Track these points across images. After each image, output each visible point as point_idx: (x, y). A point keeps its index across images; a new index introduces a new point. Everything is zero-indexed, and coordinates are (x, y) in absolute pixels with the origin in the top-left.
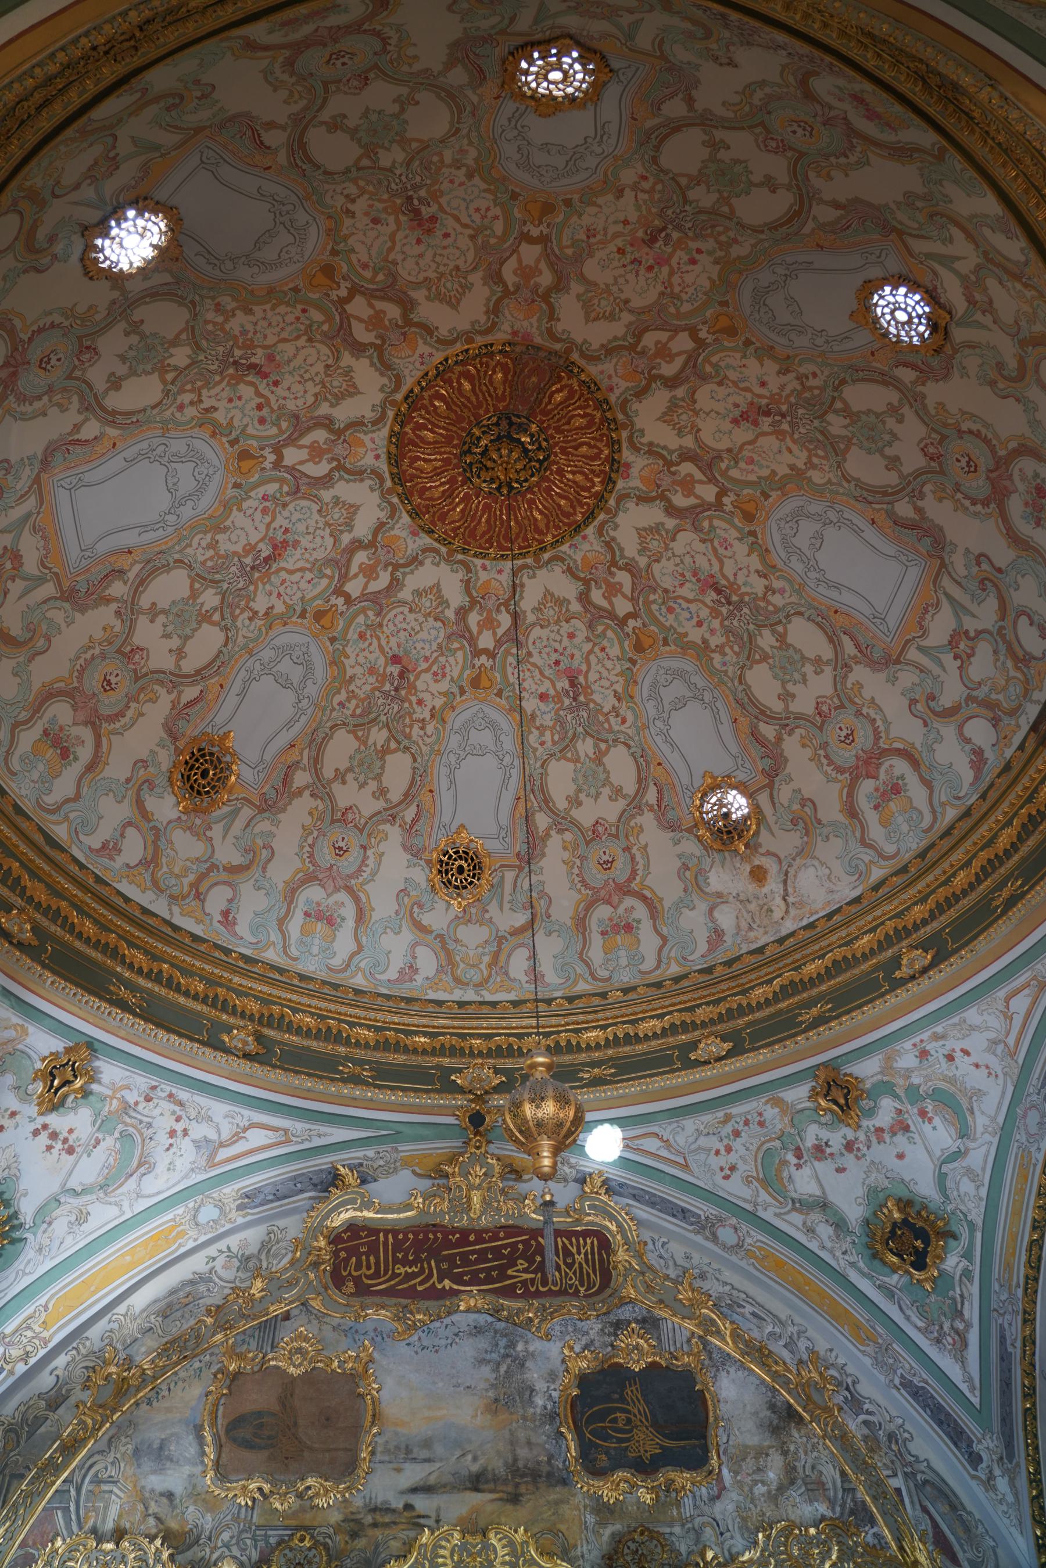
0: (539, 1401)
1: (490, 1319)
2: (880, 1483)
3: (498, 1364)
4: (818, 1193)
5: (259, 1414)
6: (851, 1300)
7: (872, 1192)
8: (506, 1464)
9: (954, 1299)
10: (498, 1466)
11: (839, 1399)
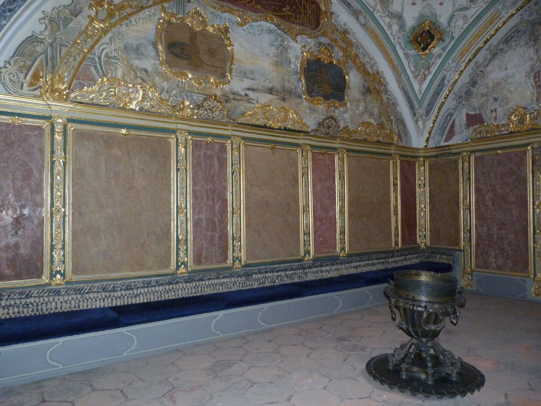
0: (292, 66)
1: (275, 28)
2: (389, 116)
3: (278, 48)
4: (400, 11)
5: (182, 44)
6: (394, 56)
7: (422, 16)
8: (281, 86)
9: (429, 63)
10: (278, 86)
11: (382, 89)
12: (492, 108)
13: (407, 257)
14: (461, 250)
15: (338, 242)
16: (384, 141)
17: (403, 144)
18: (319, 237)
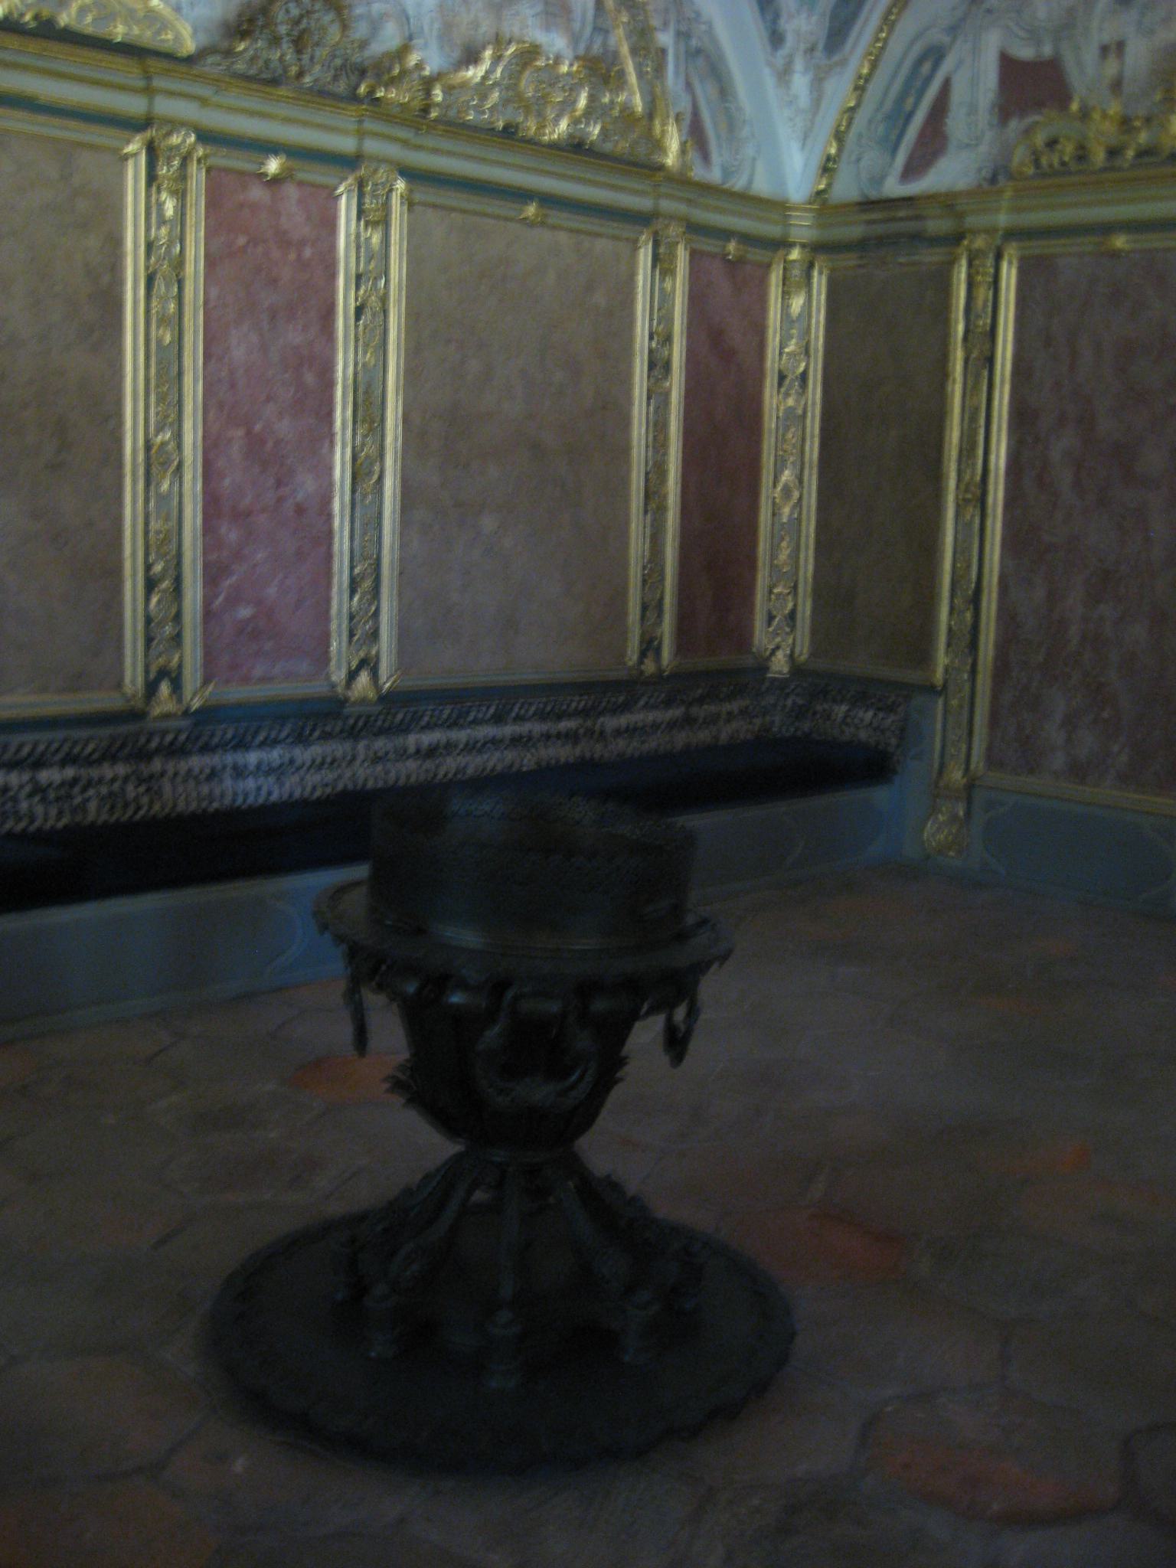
12: (1106, 38)
13: (695, 711)
14: (931, 690)
15: (338, 626)
16: (608, 147)
17: (715, 176)
18: (234, 600)
